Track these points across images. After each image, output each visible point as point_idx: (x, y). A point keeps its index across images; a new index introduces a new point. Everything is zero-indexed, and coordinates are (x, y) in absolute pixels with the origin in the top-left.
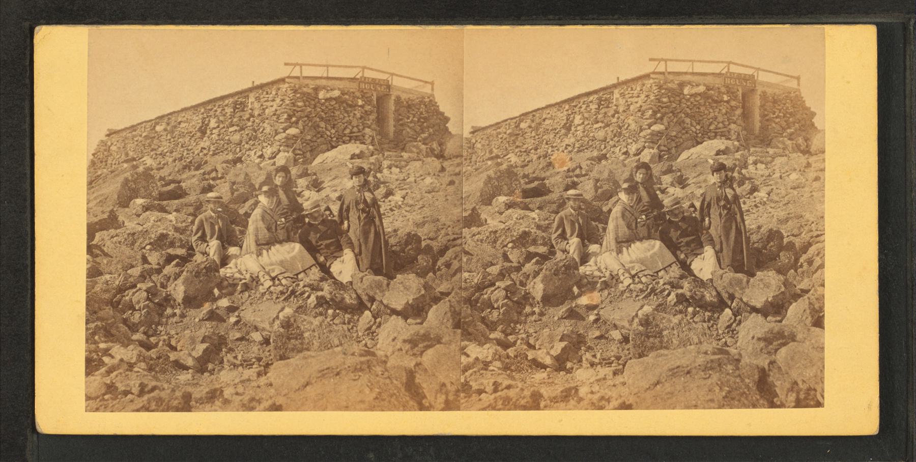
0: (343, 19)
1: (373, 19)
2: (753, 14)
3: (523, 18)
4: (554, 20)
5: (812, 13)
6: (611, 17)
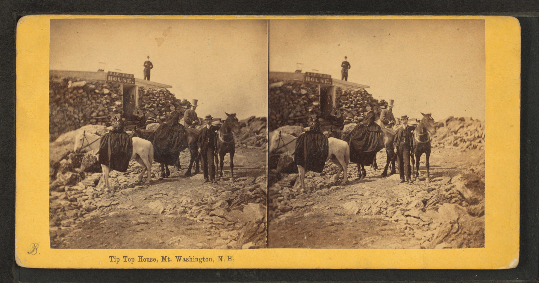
0: (204, 12)
1: (221, 12)
2: (449, 11)
5: (484, 11)
6: (364, 12)
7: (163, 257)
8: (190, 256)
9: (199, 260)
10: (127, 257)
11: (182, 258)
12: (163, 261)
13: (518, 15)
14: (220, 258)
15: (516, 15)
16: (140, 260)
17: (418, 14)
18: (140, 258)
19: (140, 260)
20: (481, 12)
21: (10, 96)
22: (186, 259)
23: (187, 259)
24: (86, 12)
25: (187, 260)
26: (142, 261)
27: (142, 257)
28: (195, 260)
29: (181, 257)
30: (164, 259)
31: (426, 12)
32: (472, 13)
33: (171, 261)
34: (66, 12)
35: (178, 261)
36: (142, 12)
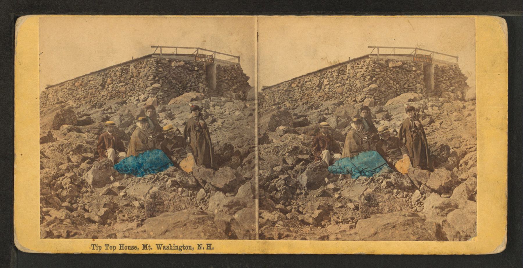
7: (144, 245)
8: (170, 245)
9: (179, 248)
10: (109, 245)
11: (162, 246)
12: (143, 249)
13: (504, 15)
14: (200, 247)
15: (502, 15)
16: (122, 248)
18: (122, 246)
19: (122, 248)
22: (166, 247)
23: (168, 247)
25: (168, 249)
26: (123, 249)
27: (123, 245)
28: (175, 248)
29: (162, 245)
30: (145, 247)
33: (152, 249)
35: (158, 249)
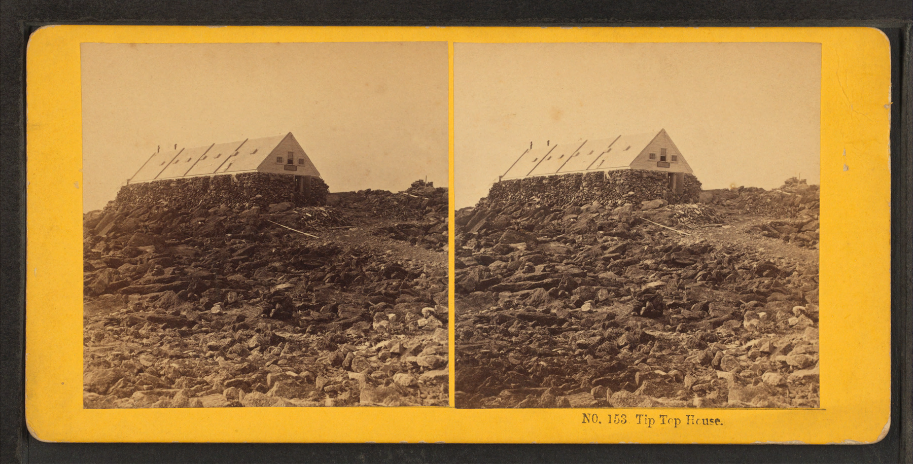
3: (517, 20)
4: (549, 22)
5: (808, 18)
6: (606, 20)
17: (697, 22)
20: (803, 19)
21: (13, 160)
24: (140, 19)
31: (710, 20)
32: (789, 20)
34: (107, 19)
36: (233, 20)
